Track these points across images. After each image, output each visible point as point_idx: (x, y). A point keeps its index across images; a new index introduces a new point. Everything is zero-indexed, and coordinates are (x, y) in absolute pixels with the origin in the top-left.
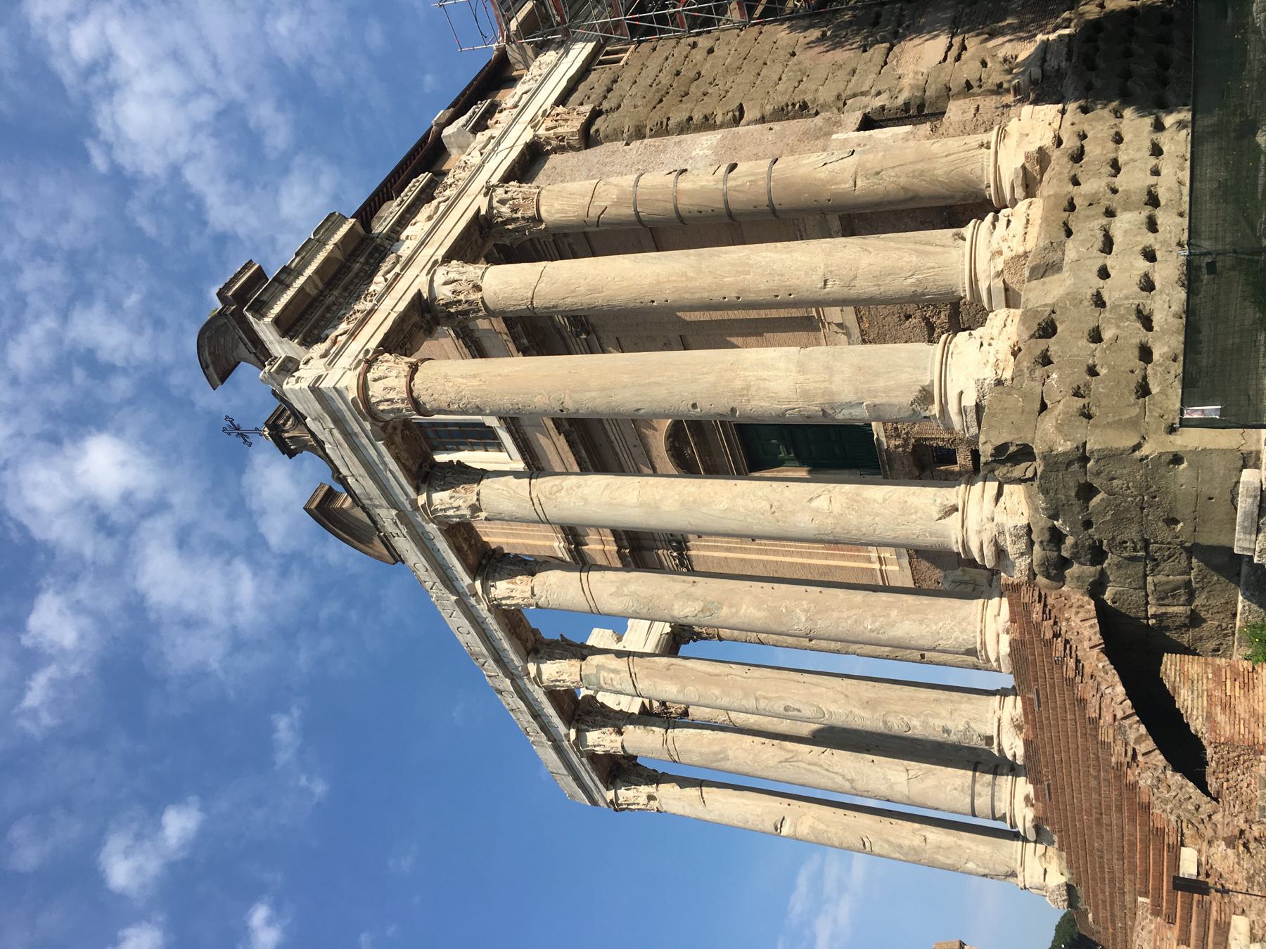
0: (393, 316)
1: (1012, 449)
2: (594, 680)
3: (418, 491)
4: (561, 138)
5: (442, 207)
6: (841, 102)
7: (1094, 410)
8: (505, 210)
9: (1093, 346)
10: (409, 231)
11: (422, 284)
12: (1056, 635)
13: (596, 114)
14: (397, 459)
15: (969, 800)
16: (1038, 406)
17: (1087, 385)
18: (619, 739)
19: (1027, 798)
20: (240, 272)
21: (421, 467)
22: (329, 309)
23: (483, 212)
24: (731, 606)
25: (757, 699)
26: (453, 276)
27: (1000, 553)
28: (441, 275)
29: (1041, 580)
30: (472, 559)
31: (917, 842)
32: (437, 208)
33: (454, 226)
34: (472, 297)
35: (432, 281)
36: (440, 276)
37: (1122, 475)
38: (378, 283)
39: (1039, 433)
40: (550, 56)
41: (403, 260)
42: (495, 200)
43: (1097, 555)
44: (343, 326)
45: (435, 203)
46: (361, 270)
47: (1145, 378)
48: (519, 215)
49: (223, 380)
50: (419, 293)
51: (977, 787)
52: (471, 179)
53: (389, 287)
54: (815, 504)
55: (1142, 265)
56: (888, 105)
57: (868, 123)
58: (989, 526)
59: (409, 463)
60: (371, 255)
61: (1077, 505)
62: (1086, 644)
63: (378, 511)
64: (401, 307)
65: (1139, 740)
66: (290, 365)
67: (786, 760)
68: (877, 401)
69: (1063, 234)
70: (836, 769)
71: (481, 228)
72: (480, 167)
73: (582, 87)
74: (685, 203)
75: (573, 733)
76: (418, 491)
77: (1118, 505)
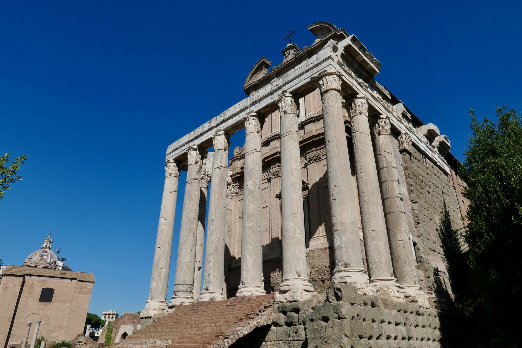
0: (352, 85)
1: (339, 294)
2: (218, 154)
3: (291, 93)
4: (403, 143)
6: (420, 236)
7: (354, 321)
8: (383, 123)
12: (260, 311)
13: (410, 154)
14: (303, 86)
15: (181, 283)
17: (360, 319)
18: (194, 163)
19: (183, 303)
21: (299, 94)
22: (352, 63)
23: (381, 116)
24: (253, 201)
25: (215, 210)
26: (364, 105)
27: (285, 292)
28: (364, 101)
29: (277, 306)
30: (263, 111)
31: (161, 266)
33: (377, 106)
37: (334, 331)
38: (360, 80)
39: (345, 303)
43: (289, 324)
44: (347, 68)
47: (364, 338)
48: (381, 128)
50: (358, 94)
51: (186, 286)
52: (390, 112)
53: (359, 84)
54: (297, 228)
55: (393, 336)
56: (421, 251)
57: (415, 244)
58: (296, 287)
59: (301, 90)
61: (320, 316)
62: (258, 321)
63: (281, 80)
64: (354, 88)
65: (232, 340)
67: (190, 221)
68: (343, 248)
69: (398, 309)
70: (189, 238)
71: (375, 115)
72: (393, 115)
75: (196, 147)
76: (291, 93)
77: (321, 330)
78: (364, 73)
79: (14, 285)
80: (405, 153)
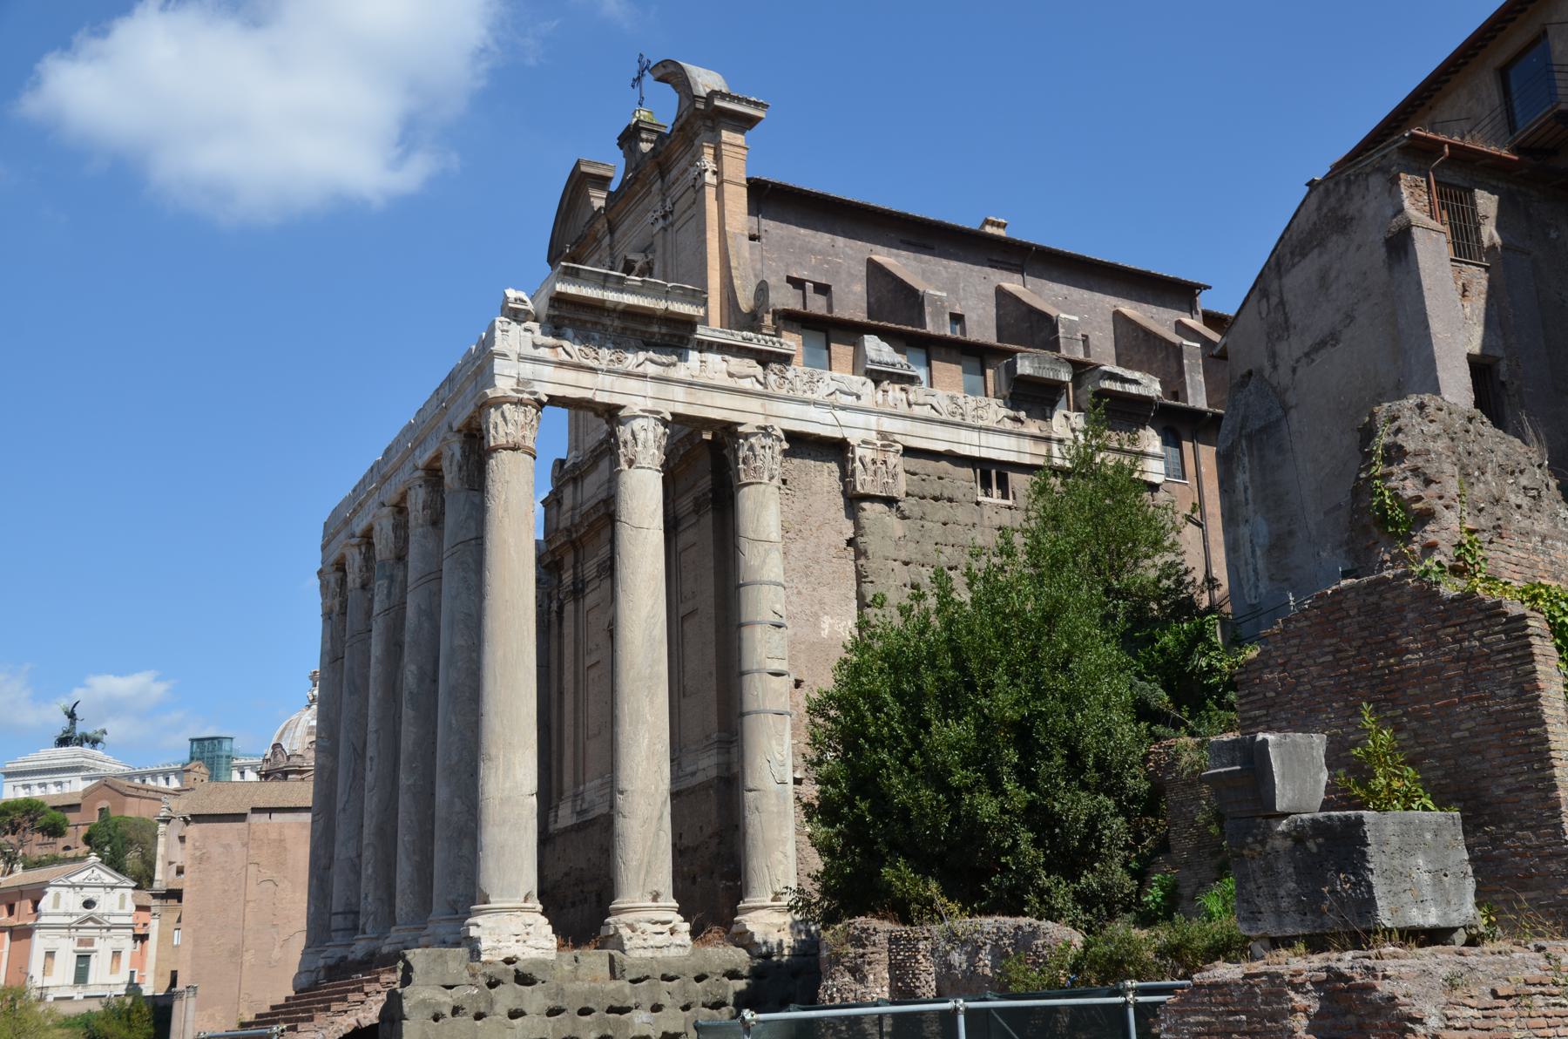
0: (588, 394)
5: (747, 384)
9: (505, 1013)
10: (713, 359)
11: (634, 405)
13: (890, 501)
16: (449, 983)
19: (345, 958)
20: (749, 102)
23: (740, 429)
26: (641, 436)
32: (748, 376)
33: (716, 407)
34: (622, 460)
35: (635, 417)
36: (637, 424)
38: (632, 360)
40: (995, 411)
41: (673, 373)
42: (753, 440)
46: (653, 335)
48: (741, 466)
49: (659, 80)
53: (628, 374)
62: (361, 1015)
66: (521, 316)
69: (634, 977)
73: (944, 464)
74: (746, 631)
76: (459, 431)
78: (655, 329)
79: (227, 847)
80: (866, 505)
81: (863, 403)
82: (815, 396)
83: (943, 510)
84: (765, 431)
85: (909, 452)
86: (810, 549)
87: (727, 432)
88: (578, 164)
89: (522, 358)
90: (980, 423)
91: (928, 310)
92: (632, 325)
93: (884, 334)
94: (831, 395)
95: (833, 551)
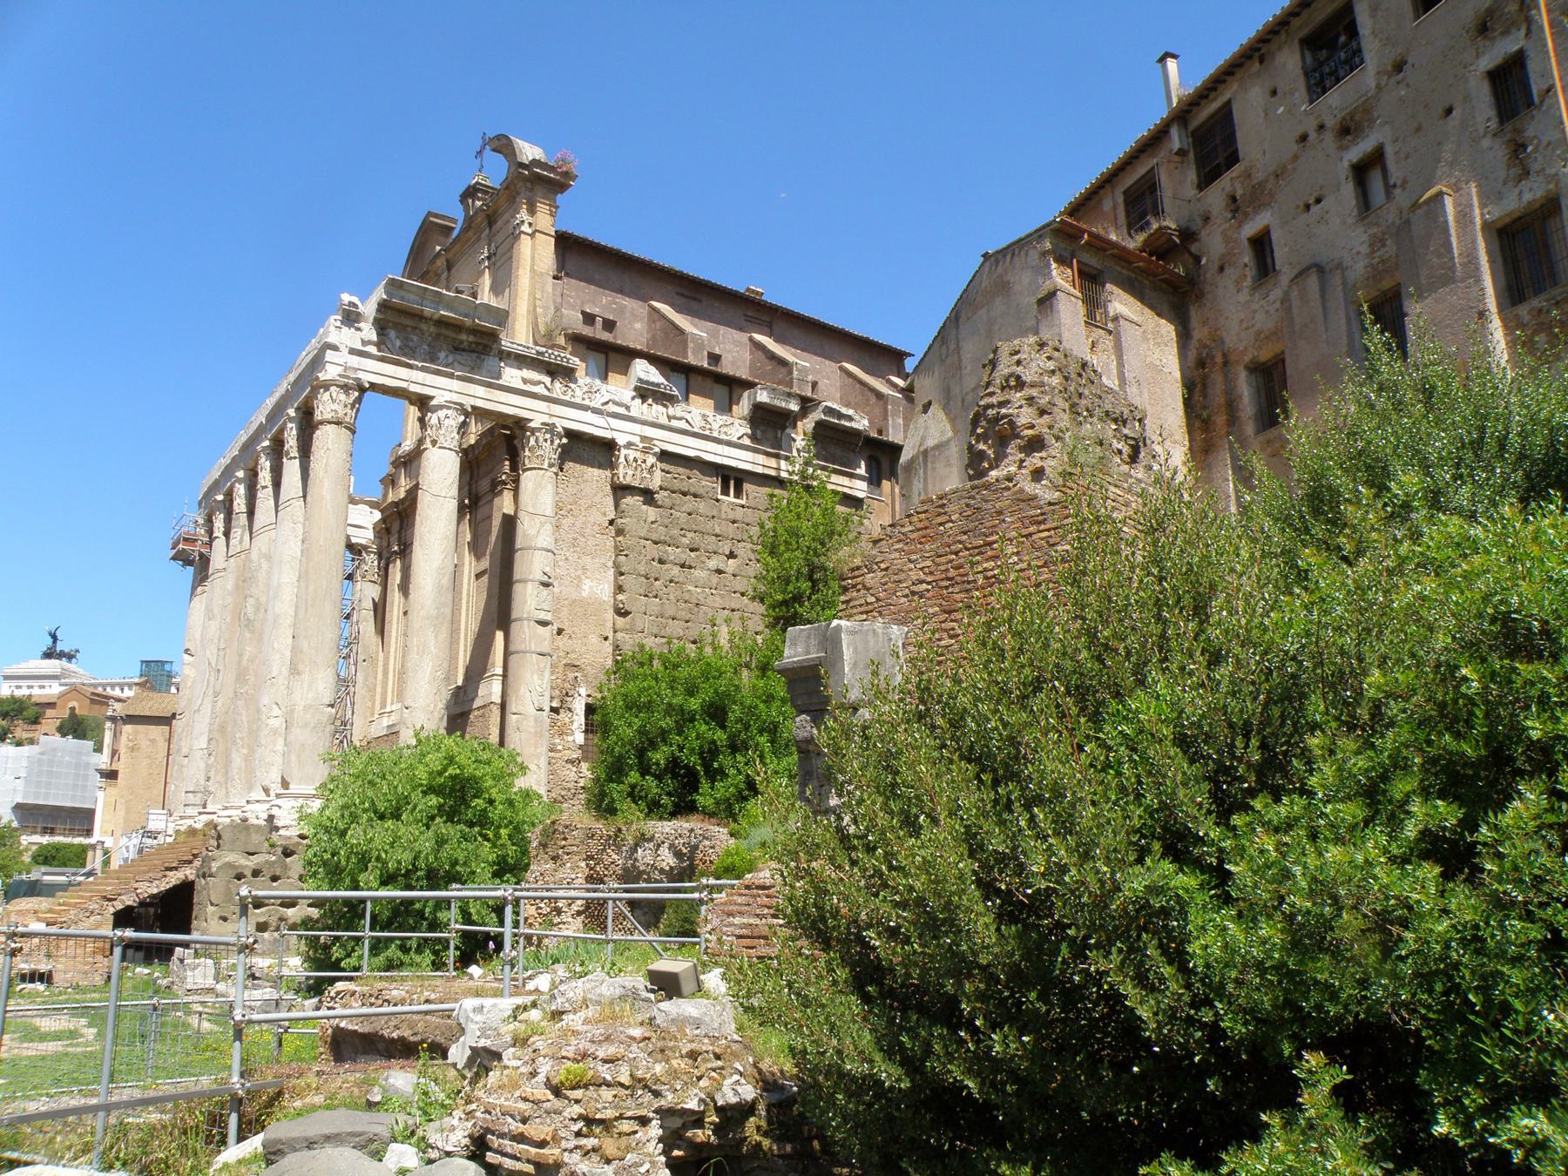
0: (404, 385)
8: (532, 441)
11: (440, 398)
22: (414, 328)
32: (539, 383)
35: (441, 407)
36: (442, 413)
45: (547, 380)
46: (462, 342)
50: (432, 398)
60: (477, 344)
64: (413, 388)
78: (464, 337)
81: (634, 413)
82: (592, 405)
83: (690, 503)
84: (550, 428)
85: (665, 456)
86: (578, 525)
87: (519, 425)
88: (429, 214)
89: (353, 351)
90: (723, 437)
91: (691, 345)
92: (444, 331)
93: (654, 360)
94: (606, 403)
95: (596, 528)
